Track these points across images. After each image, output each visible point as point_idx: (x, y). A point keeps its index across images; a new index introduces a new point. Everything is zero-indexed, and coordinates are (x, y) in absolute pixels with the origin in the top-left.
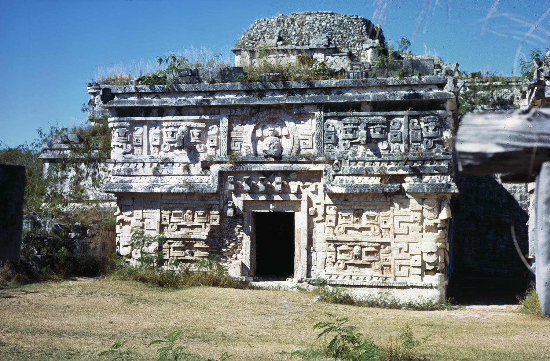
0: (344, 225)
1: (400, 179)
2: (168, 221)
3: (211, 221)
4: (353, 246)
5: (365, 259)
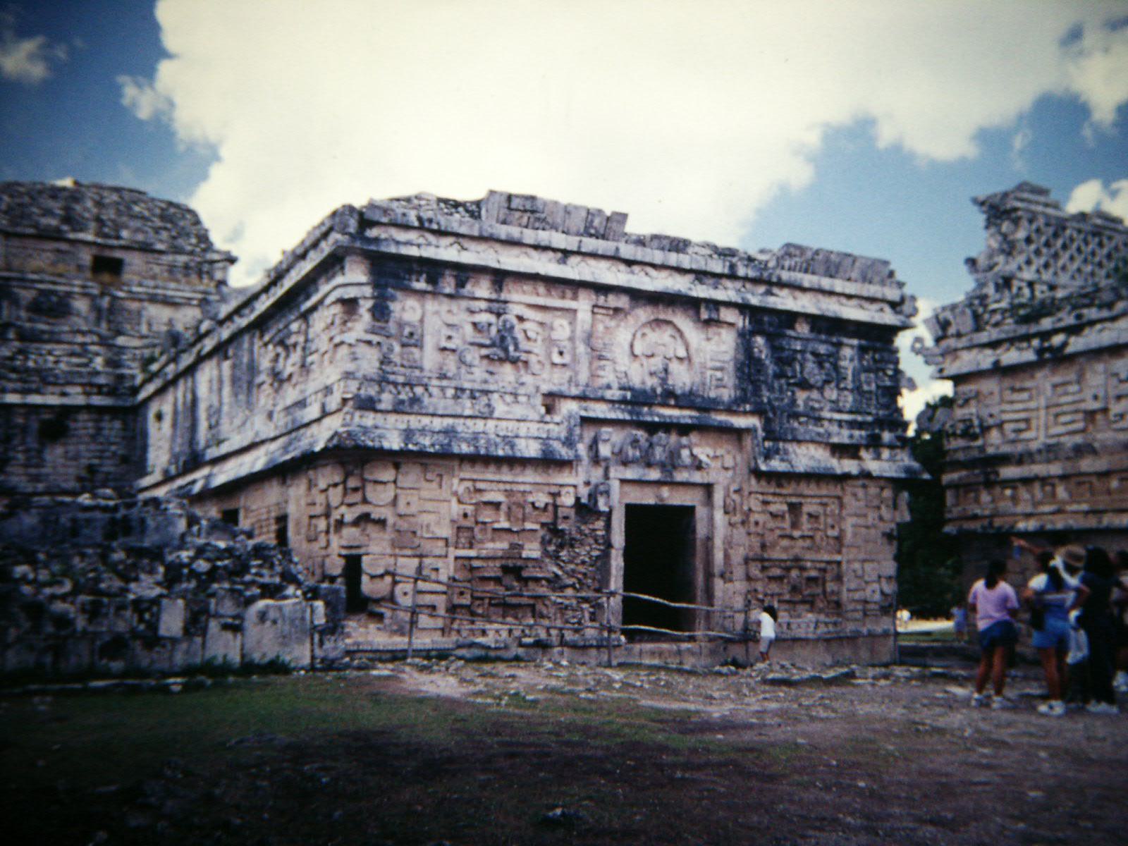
3: (560, 521)
4: (788, 569)
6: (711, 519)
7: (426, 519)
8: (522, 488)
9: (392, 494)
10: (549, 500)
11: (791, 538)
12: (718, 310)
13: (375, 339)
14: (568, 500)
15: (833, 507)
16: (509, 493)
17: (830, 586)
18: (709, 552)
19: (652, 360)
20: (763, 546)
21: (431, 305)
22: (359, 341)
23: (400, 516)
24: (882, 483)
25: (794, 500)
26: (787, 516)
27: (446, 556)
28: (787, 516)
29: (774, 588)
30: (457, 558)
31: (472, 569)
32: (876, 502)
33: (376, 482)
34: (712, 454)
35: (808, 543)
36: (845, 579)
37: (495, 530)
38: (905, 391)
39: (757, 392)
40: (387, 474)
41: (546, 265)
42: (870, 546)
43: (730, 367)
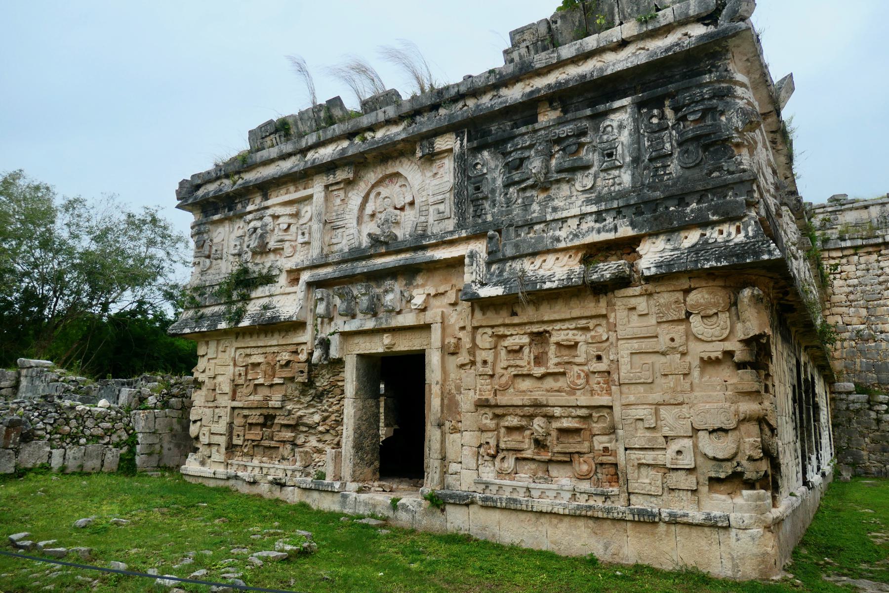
0: (510, 369)
2: (243, 377)
4: (531, 417)
5: (556, 447)
12: (432, 144)
14: (303, 357)
24: (685, 284)
25: (535, 329)
26: (526, 350)
30: (233, 408)
31: (245, 417)
34: (433, 293)
35: (561, 383)
36: (620, 432)
37: (256, 385)
41: (286, 166)
42: (671, 381)
43: (450, 197)
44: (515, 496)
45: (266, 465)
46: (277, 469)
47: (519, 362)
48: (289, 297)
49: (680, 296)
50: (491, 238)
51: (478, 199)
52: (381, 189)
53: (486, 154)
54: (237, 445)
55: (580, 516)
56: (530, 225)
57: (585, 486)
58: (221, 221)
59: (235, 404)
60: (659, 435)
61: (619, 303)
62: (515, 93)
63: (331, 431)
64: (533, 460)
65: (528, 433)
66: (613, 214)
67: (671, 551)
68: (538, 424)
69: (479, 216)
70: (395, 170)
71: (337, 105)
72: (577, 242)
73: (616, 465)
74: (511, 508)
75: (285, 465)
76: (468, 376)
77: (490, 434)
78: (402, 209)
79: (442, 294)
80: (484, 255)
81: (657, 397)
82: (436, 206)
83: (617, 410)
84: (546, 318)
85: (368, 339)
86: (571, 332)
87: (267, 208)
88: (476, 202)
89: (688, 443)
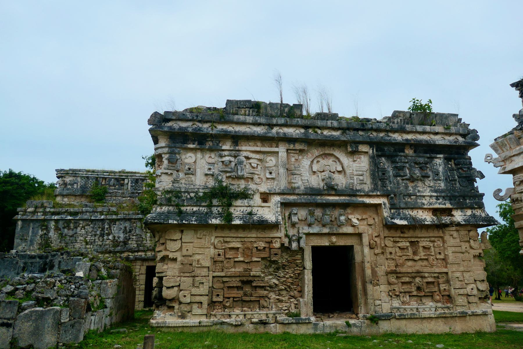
0: (403, 257)
1: (448, 212)
2: (223, 257)
3: (272, 256)
4: (414, 278)
6: (363, 252)
7: (197, 257)
8: (251, 240)
9: (180, 245)
10: (267, 245)
11: (415, 261)
12: (357, 147)
13: (169, 172)
14: (277, 245)
15: (439, 243)
16: (243, 243)
17: (443, 287)
18: (363, 270)
19: (323, 173)
20: (397, 266)
21: (199, 155)
22: (162, 173)
23: (184, 256)
24: (469, 228)
26: (410, 249)
27: (208, 276)
28: (410, 249)
29: (406, 288)
30: (213, 277)
31: (224, 282)
32: (466, 239)
33: (171, 240)
34: (360, 218)
35: (425, 263)
37: (235, 262)
38: (477, 179)
39: (384, 186)
40: (177, 236)
41: (259, 130)
42: (465, 263)
44: (411, 312)
45: (250, 313)
46: (260, 314)
47: (408, 254)
48: (264, 209)
49: (467, 232)
50: (392, 198)
51: (384, 179)
52: (319, 159)
53: (383, 159)
54: (215, 302)
55: (441, 317)
56: (410, 195)
57: (439, 305)
58: (191, 150)
59: (216, 274)
60: (463, 283)
61: (447, 232)
62: (397, 137)
63: (288, 289)
64: (417, 296)
65: (413, 284)
66: (442, 198)
67: (472, 325)
68: (418, 280)
69: (385, 187)
70: (331, 152)
71: (299, 108)
72: (431, 207)
73: (449, 296)
74: (412, 318)
75: (265, 311)
76: (381, 259)
77: (396, 286)
78: (334, 173)
79: (364, 219)
80: (388, 205)
81: (462, 269)
82: (357, 177)
83: (450, 274)
84: (419, 236)
85: (318, 238)
86: (428, 242)
87: (240, 151)
88: (382, 180)
89: (473, 286)
